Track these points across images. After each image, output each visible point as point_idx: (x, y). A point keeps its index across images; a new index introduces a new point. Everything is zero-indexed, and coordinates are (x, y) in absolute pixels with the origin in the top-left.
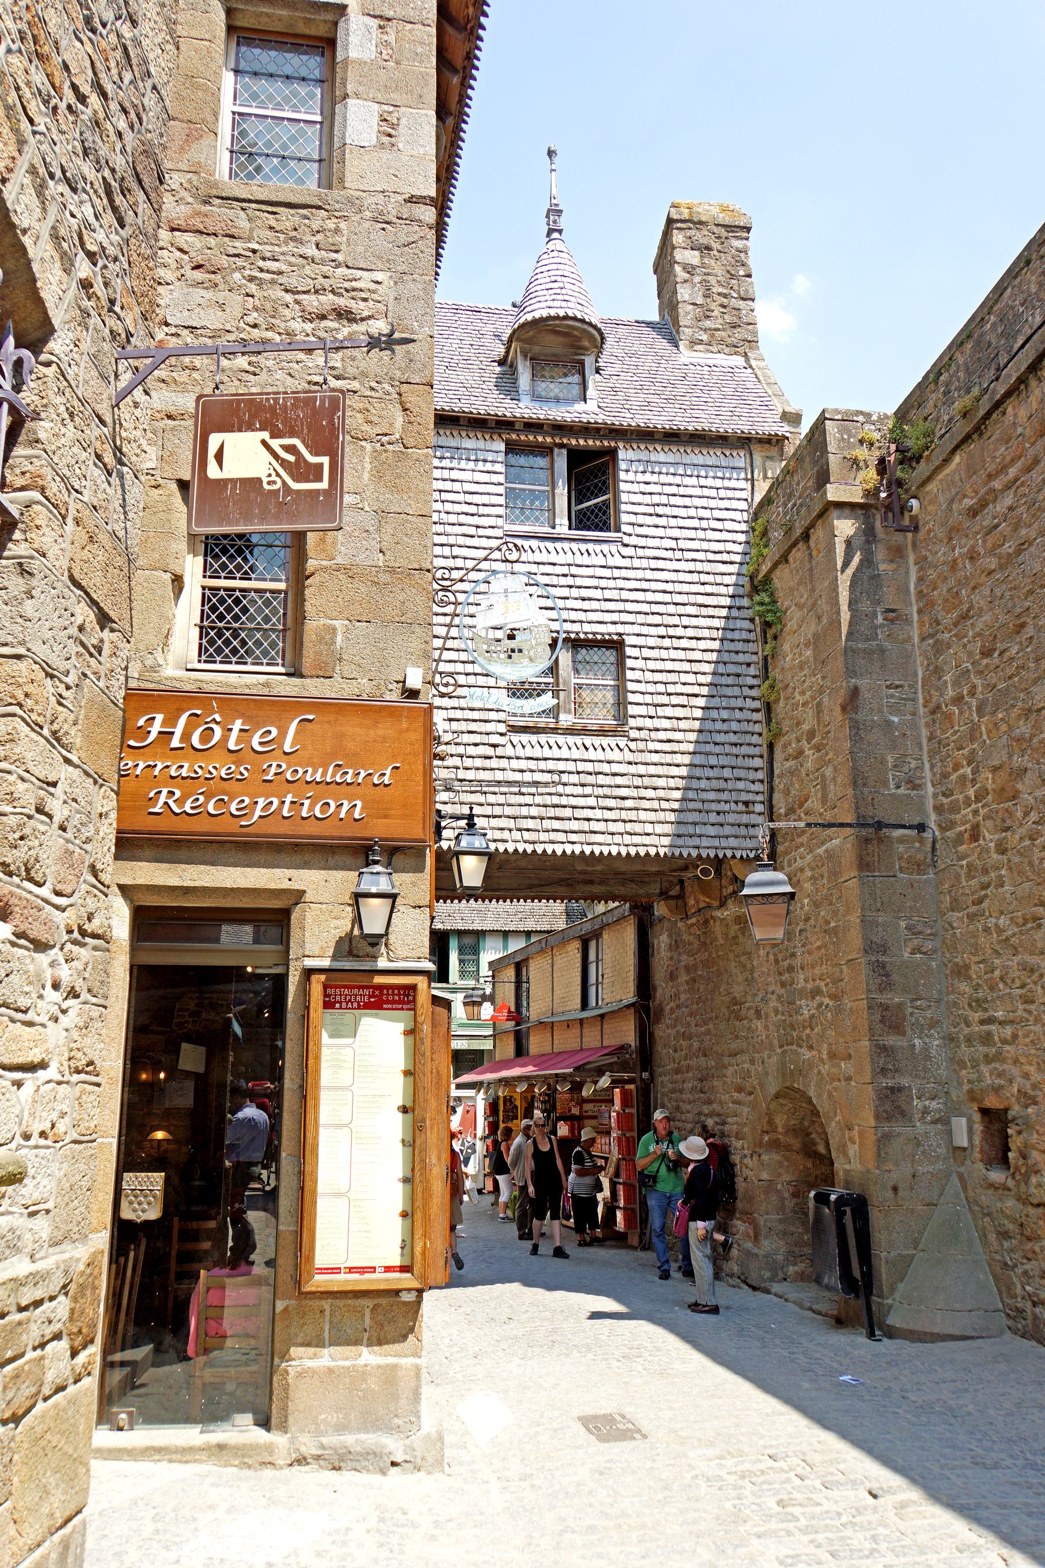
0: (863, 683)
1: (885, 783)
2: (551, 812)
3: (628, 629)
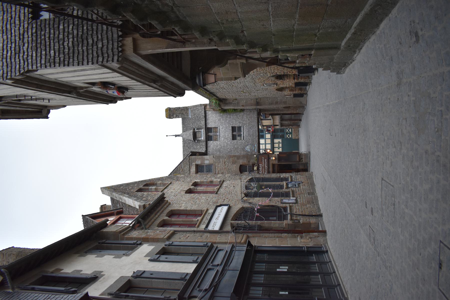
2: (253, 135)
3: (230, 126)
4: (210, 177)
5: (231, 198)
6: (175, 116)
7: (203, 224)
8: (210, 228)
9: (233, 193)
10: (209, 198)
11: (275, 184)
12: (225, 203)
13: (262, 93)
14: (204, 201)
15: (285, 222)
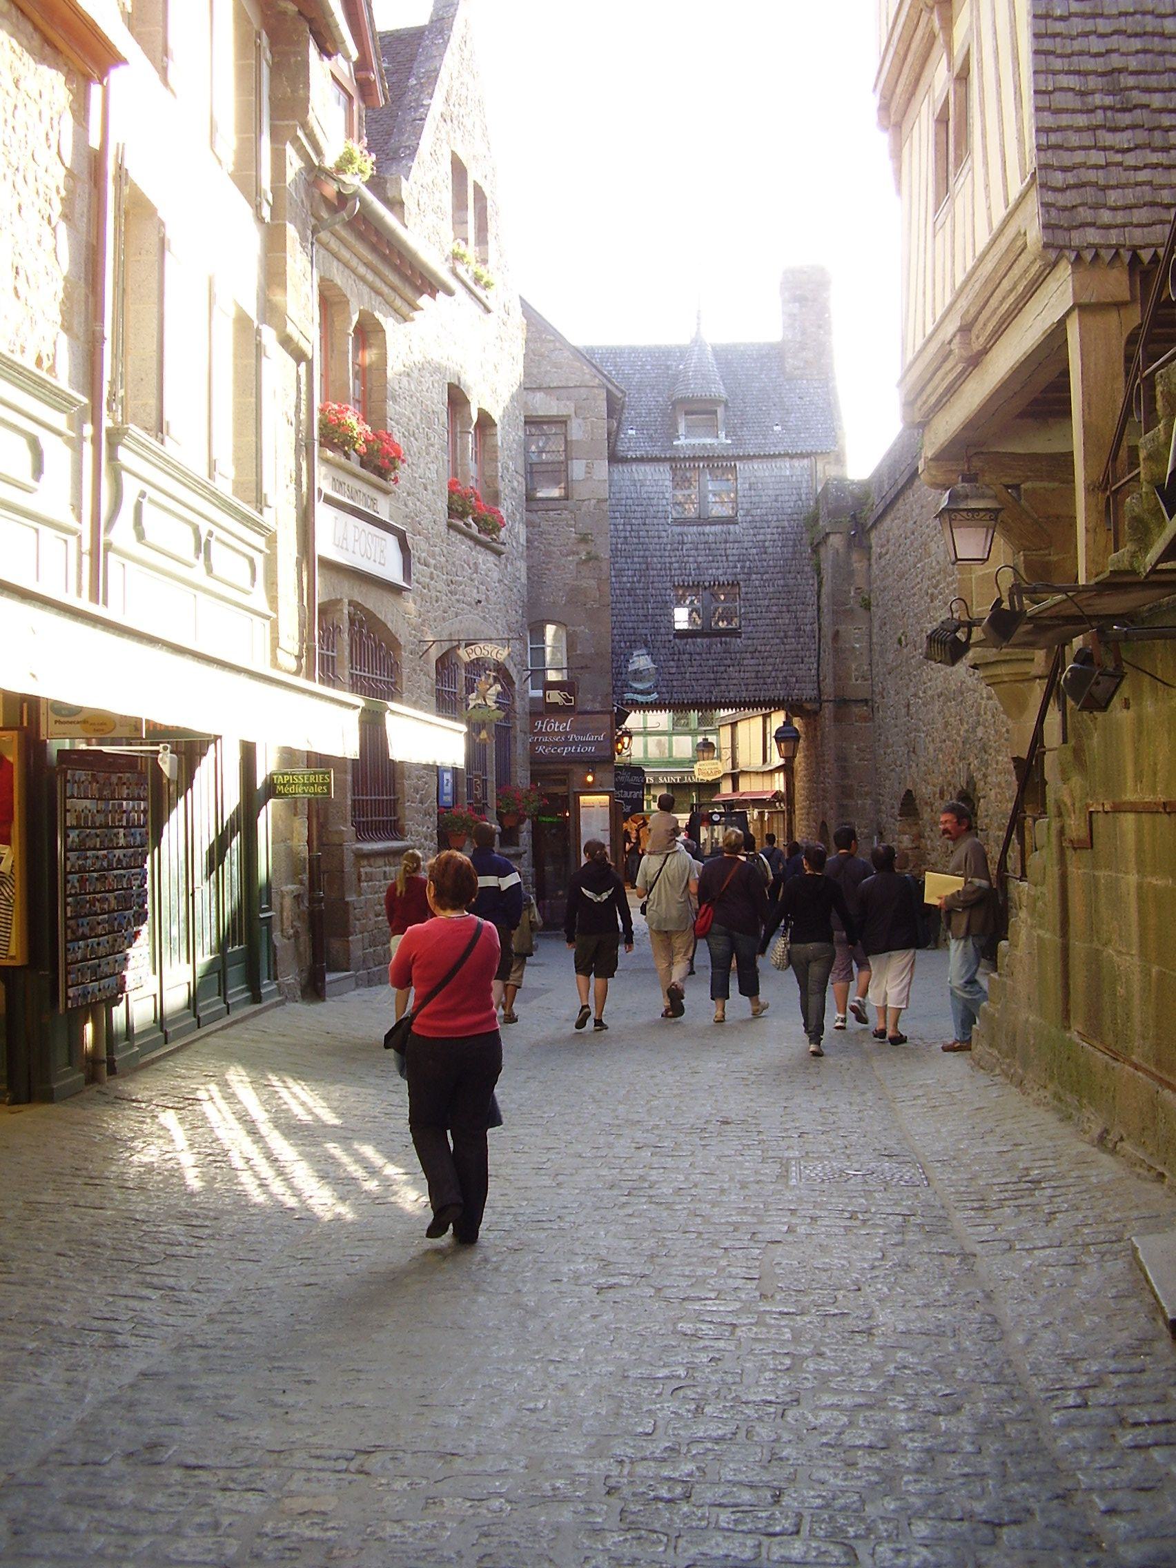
0: (842, 628)
1: (850, 679)
4: (513, 490)
5: (434, 594)
6: (795, 307)
7: (334, 479)
8: (324, 515)
9: (453, 598)
10: (434, 493)
11: (488, 785)
12: (416, 567)
13: (896, 726)
14: (420, 471)
15: (348, 829)
